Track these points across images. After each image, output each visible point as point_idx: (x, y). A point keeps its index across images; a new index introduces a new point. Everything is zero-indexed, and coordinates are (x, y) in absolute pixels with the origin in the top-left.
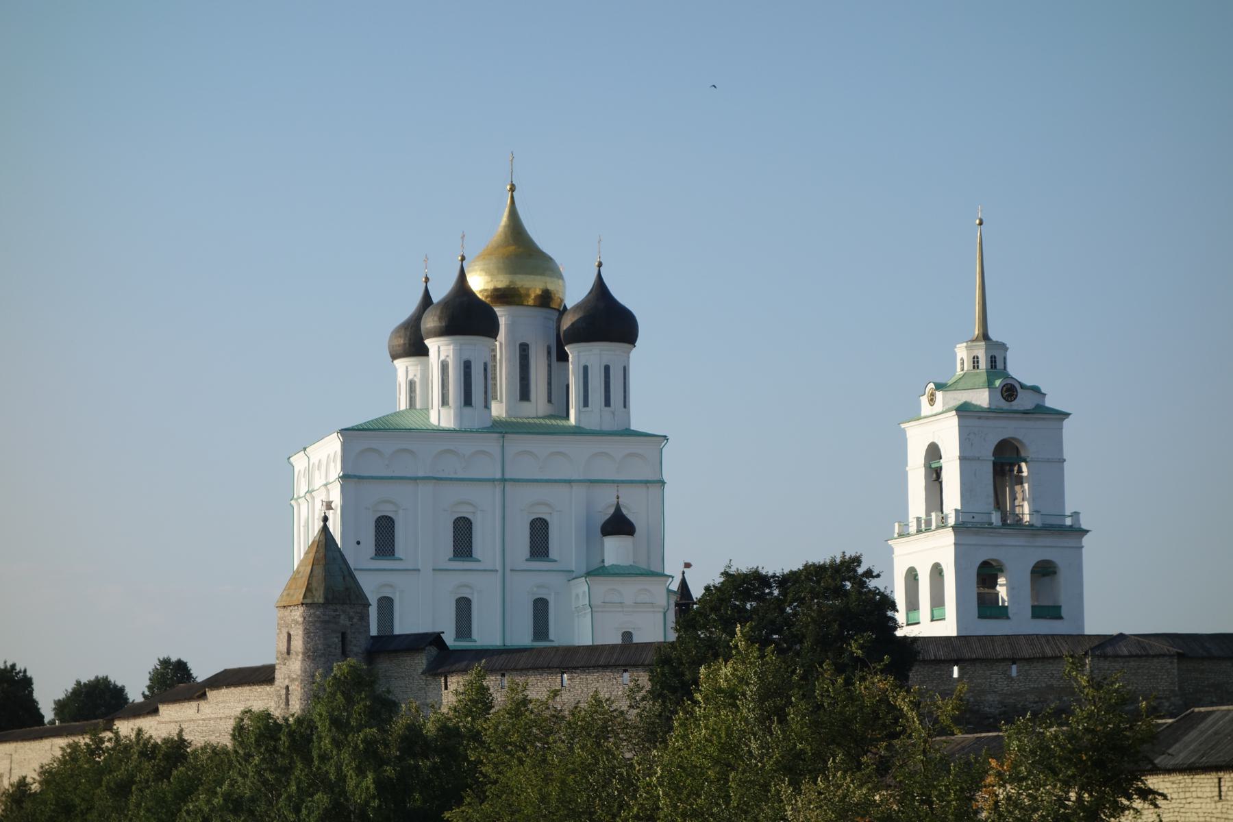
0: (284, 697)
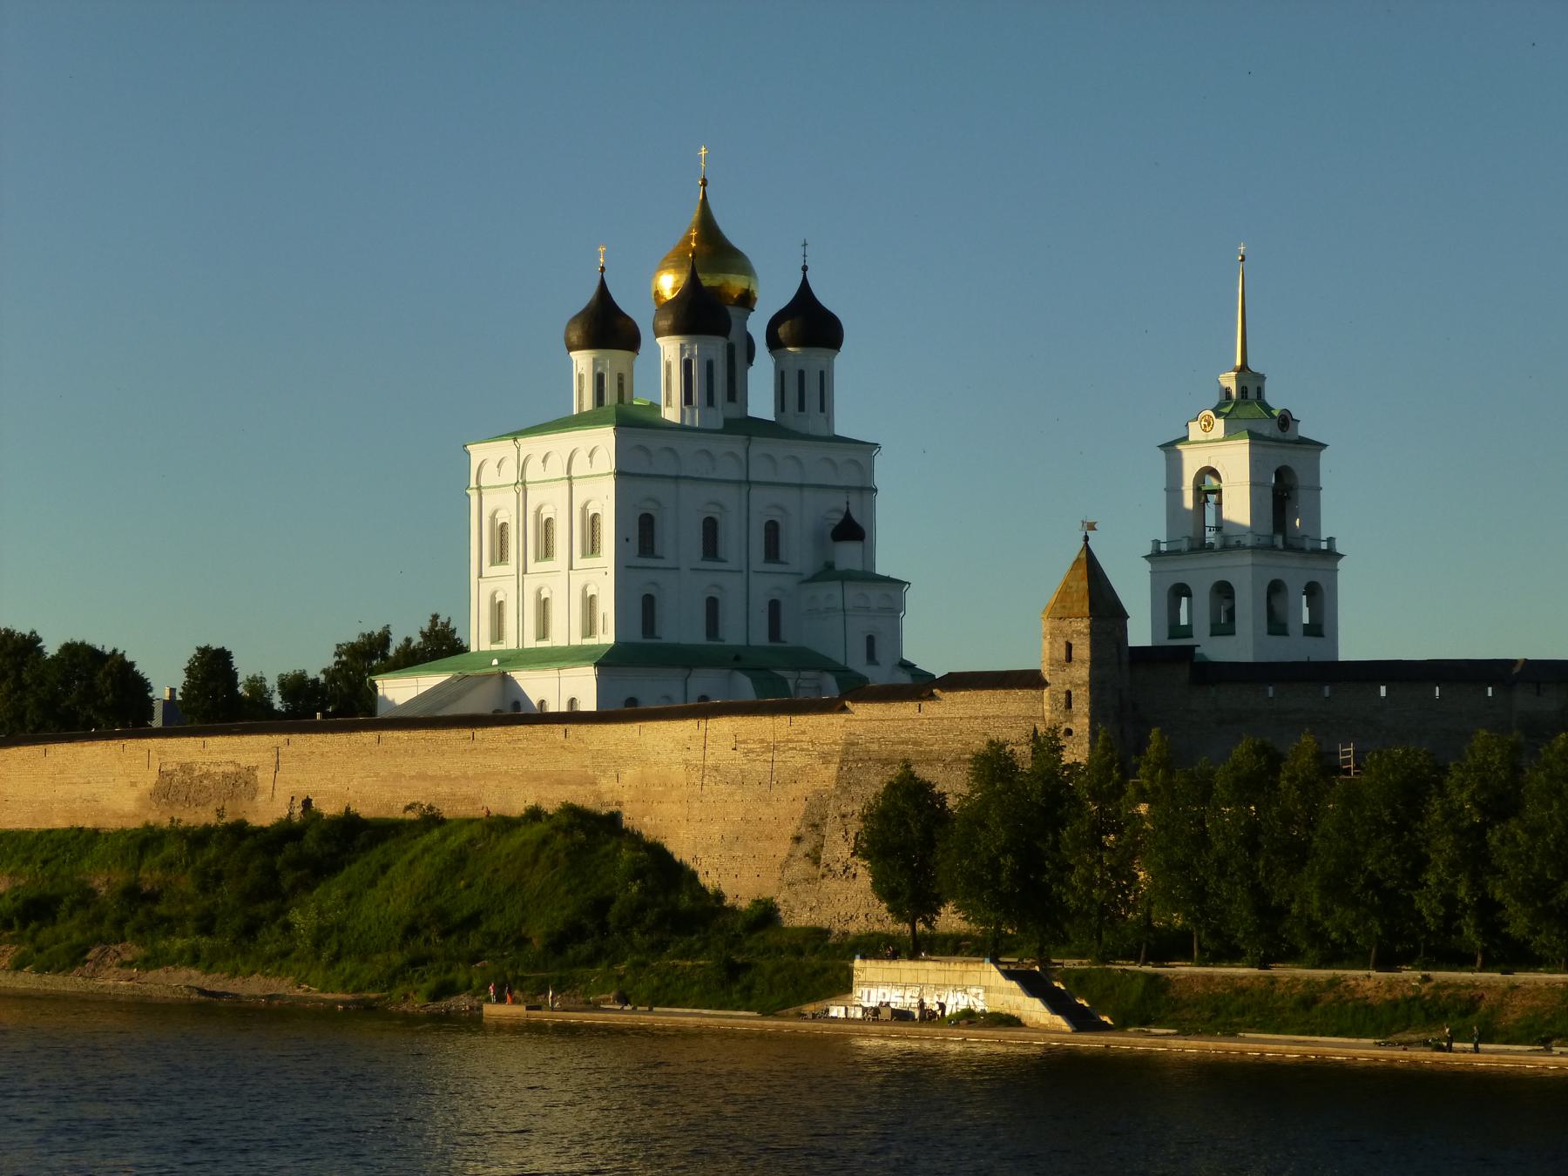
0: (1063, 701)
